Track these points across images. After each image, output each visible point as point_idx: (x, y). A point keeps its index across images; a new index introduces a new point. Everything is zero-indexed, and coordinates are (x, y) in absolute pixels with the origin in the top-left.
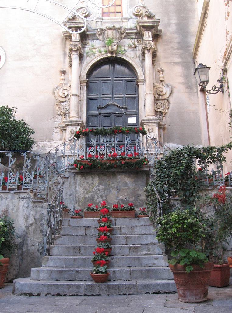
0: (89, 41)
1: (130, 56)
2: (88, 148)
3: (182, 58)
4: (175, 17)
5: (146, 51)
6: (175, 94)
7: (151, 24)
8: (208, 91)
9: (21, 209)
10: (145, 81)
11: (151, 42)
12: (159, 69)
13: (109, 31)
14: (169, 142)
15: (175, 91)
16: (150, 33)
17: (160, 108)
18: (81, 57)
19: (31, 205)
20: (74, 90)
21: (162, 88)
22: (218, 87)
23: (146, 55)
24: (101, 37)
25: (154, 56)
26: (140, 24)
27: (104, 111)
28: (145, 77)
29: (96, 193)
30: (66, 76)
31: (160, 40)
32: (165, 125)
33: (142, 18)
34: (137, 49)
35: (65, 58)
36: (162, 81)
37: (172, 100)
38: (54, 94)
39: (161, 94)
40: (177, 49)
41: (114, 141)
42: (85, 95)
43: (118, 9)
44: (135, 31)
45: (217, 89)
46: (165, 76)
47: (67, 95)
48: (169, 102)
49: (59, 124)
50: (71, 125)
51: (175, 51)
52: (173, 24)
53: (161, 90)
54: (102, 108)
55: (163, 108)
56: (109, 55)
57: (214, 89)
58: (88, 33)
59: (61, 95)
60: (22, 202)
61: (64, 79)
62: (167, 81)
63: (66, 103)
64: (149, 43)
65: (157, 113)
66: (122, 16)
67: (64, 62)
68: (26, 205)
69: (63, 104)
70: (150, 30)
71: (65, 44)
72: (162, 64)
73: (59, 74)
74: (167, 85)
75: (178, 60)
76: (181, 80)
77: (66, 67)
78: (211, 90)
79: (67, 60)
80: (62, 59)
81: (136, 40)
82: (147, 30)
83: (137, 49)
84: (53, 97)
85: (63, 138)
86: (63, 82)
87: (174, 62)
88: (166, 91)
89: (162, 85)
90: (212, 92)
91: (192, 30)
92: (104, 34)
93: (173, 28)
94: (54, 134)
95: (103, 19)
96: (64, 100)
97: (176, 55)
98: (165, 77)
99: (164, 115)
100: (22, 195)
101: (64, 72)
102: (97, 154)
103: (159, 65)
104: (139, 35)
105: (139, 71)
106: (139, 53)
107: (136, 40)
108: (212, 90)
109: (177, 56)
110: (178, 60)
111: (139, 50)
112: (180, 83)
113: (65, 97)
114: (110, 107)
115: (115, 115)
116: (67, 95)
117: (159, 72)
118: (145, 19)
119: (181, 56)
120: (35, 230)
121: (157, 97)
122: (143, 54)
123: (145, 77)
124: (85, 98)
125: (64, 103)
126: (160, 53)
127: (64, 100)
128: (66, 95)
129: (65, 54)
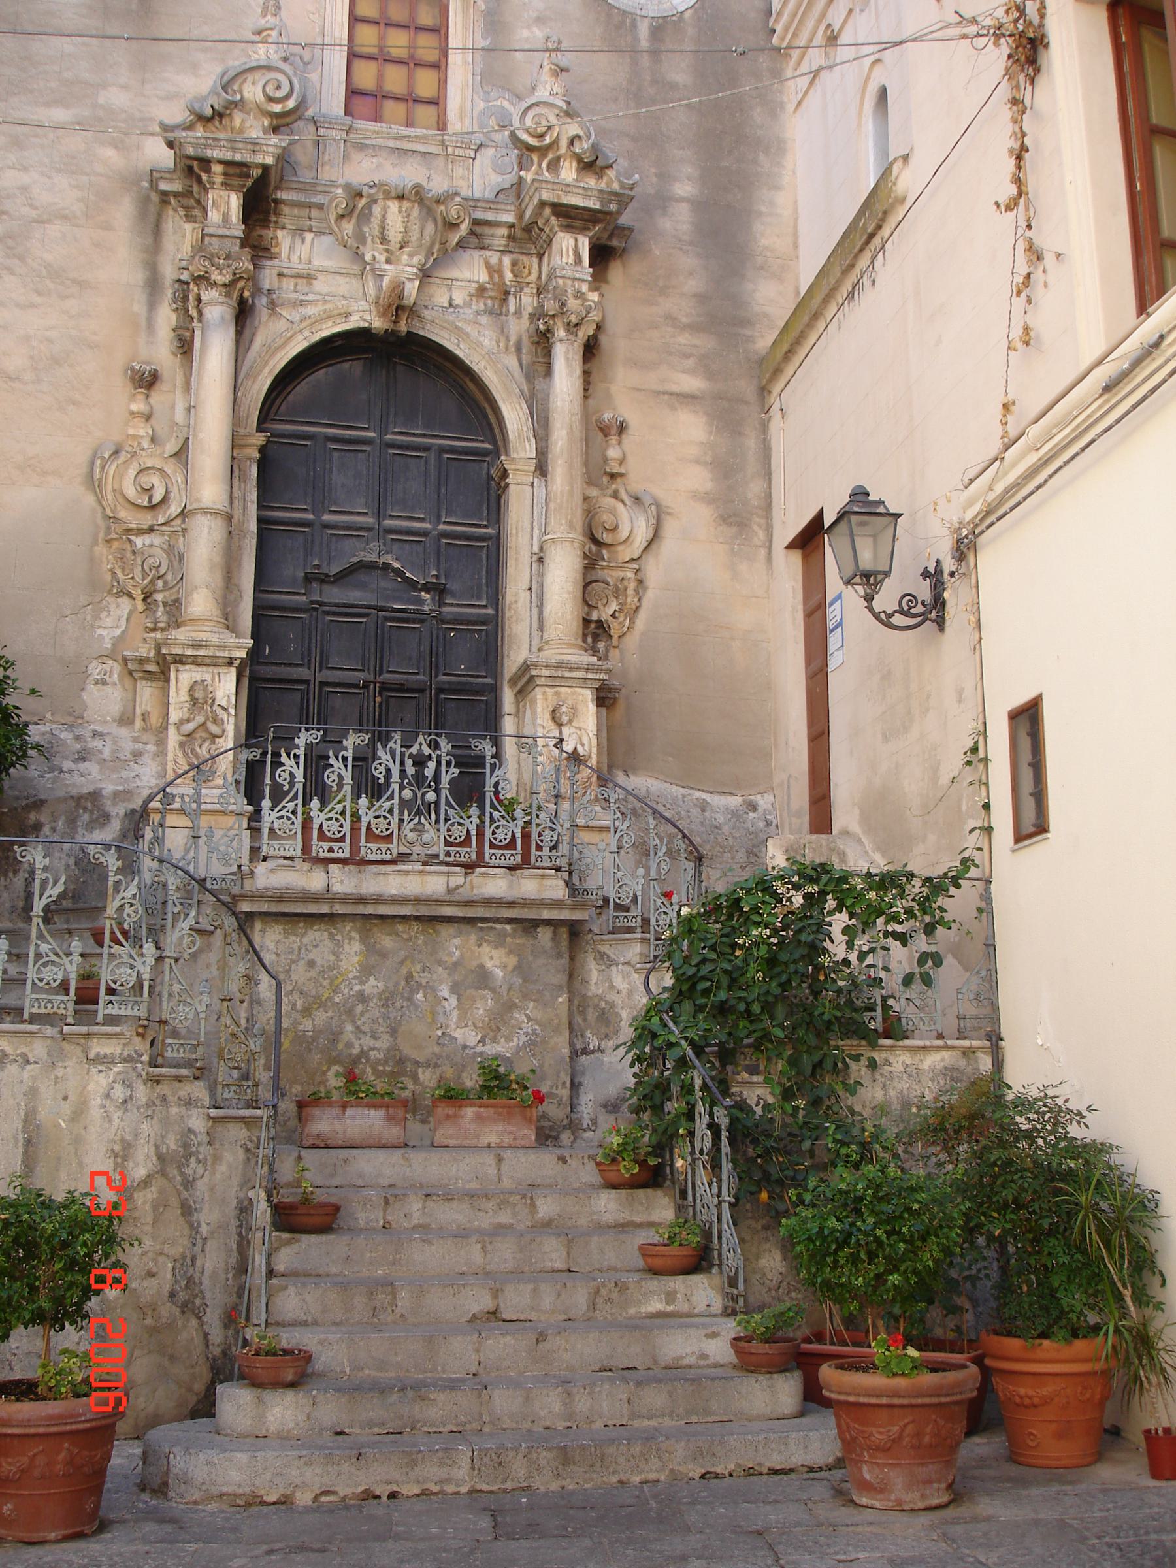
0: (280, 234)
1: (482, 345)
2: (315, 803)
3: (710, 375)
4: (688, 170)
5: (561, 333)
6: (669, 545)
7: (593, 204)
8: (883, 616)
9: (95, 1113)
10: (542, 469)
11: (585, 288)
12: (606, 416)
13: (393, 206)
15: (670, 528)
17: (601, 607)
18: (243, 314)
19: (142, 1092)
21: (613, 512)
22: (923, 603)
24: (348, 227)
26: (546, 196)
27: (334, 594)
29: (350, 1012)
30: (158, 398)
32: (618, 690)
33: (554, 166)
34: (512, 309)
35: (152, 305)
36: (613, 476)
37: (654, 571)
38: (93, 483)
39: (606, 538)
40: (693, 328)
41: (437, 777)
42: (253, 509)
43: (425, 83)
44: (509, 218)
45: (919, 609)
46: (635, 456)
47: (165, 500)
49: (118, 641)
50: (196, 662)
51: (684, 339)
52: (682, 200)
54: (324, 579)
55: (614, 606)
57: (906, 608)
58: (282, 195)
59: (131, 492)
60: (99, 1081)
61: (148, 417)
62: (637, 477)
63: (157, 539)
64: (579, 295)
66: (442, 125)
68: (119, 1093)
69: (139, 541)
70: (583, 230)
71: (157, 231)
72: (623, 396)
73: (120, 386)
74: (637, 499)
76: (699, 479)
78: (896, 611)
79: (166, 317)
80: (139, 307)
81: (507, 261)
82: (569, 228)
83: (512, 309)
84: (90, 499)
85: (138, 711)
86: (142, 430)
87: (675, 388)
88: (633, 526)
89: (615, 495)
90: (898, 620)
91: (764, 242)
92: (365, 217)
94: (91, 687)
95: (350, 130)
96: (147, 520)
97: (687, 356)
98: (630, 459)
99: (615, 641)
100: (98, 1048)
102: (355, 830)
103: (609, 396)
105: (514, 417)
106: (519, 327)
107: (507, 261)
108: (900, 611)
109: (690, 362)
111: (518, 313)
112: (695, 496)
113: (152, 507)
114: (362, 577)
115: (387, 619)
116: (165, 500)
117: (605, 430)
118: (568, 172)
119: (706, 366)
120: (159, 1206)
122: (543, 341)
124: (253, 526)
125: (147, 539)
126: (616, 344)
127: (147, 520)
128: (157, 498)
129: (153, 284)
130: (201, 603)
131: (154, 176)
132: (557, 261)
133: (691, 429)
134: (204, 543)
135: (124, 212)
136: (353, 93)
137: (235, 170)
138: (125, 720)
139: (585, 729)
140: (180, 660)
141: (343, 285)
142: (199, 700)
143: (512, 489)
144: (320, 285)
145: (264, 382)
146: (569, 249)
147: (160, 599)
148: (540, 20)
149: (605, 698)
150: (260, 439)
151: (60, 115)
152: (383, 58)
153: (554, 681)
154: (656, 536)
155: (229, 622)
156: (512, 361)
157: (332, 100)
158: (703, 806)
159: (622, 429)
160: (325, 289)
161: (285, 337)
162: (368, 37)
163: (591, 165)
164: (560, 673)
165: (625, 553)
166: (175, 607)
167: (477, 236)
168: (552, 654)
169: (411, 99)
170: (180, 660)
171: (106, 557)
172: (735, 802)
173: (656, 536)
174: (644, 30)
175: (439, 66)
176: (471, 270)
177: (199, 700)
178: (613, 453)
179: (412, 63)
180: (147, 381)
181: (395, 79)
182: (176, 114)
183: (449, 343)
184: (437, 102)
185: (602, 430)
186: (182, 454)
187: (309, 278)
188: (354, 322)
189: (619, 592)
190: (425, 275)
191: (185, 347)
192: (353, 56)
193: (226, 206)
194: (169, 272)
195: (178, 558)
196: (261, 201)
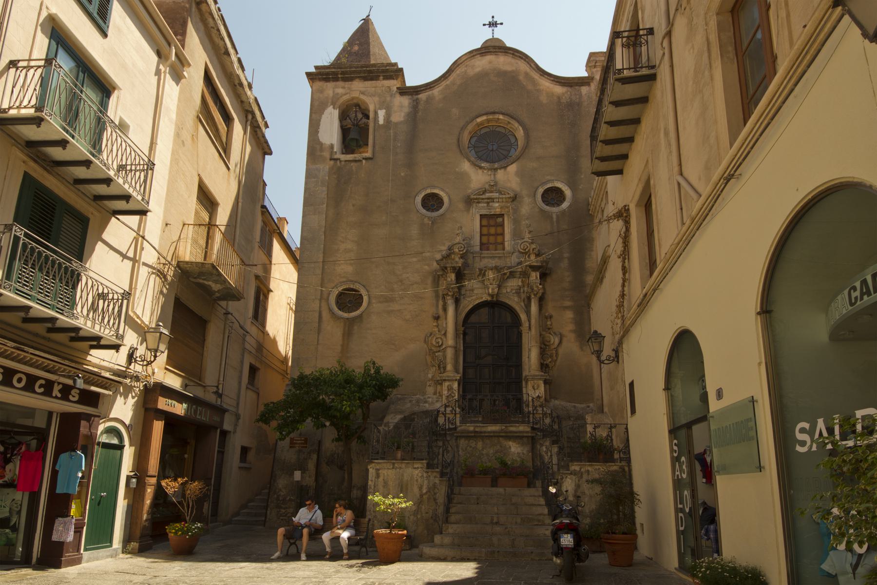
1: (515, 302)
6: (564, 344)
10: (530, 328)
14: (556, 399)
15: (565, 339)
16: (538, 274)
18: (457, 301)
20: (450, 341)
23: (533, 301)
25: (541, 300)
28: (530, 325)
31: (549, 280)
33: (529, 257)
38: (425, 341)
48: (557, 354)
49: (433, 377)
50: (449, 380)
53: (548, 339)
56: (489, 299)
63: (440, 354)
65: (543, 367)
66: (504, 249)
67: (437, 306)
72: (550, 309)
75: (568, 303)
76: (571, 327)
77: (441, 312)
79: (441, 303)
86: (436, 329)
92: (484, 275)
93: (565, 263)
101: (437, 318)
104: (525, 275)
105: (523, 317)
106: (523, 296)
110: (568, 303)
112: (571, 331)
113: (440, 346)
117: (546, 318)
121: (544, 348)
122: (529, 299)
123: (530, 325)
129: (437, 296)
130: (449, 367)
131: (436, 271)
132: (531, 279)
133: (569, 315)
134: (450, 353)
135: (430, 281)
136: (482, 244)
137: (454, 268)
138: (435, 394)
139: (541, 390)
140: (445, 380)
141: (480, 291)
142: (450, 389)
143: (523, 335)
144: (475, 292)
145: (463, 315)
146: (535, 276)
147: (442, 367)
148: (527, 219)
149: (546, 382)
150: (463, 329)
151: (415, 259)
152: (489, 235)
153: (533, 379)
154: (560, 342)
155: (456, 370)
156: (522, 304)
157: (477, 248)
158: (575, 407)
159: (551, 317)
160: (478, 292)
161: (468, 304)
162: (485, 230)
163: (538, 255)
164: (534, 378)
165: (553, 347)
166: (445, 368)
167: (512, 275)
168: (533, 373)
169: (496, 243)
170: (445, 380)
171: (429, 359)
172: (583, 406)
173: (560, 342)
174: (554, 216)
175: (503, 234)
176: (514, 283)
177: (450, 389)
178: (549, 323)
179: (496, 234)
180: (437, 318)
181: (492, 239)
182: (438, 256)
183: (507, 301)
184: (503, 243)
185: (544, 317)
186: (445, 334)
187: (473, 290)
188: (484, 299)
189: (551, 356)
190: (499, 287)
191: (445, 309)
192: (481, 235)
193: (452, 277)
194: (441, 293)
195: (445, 357)
196: (460, 276)
